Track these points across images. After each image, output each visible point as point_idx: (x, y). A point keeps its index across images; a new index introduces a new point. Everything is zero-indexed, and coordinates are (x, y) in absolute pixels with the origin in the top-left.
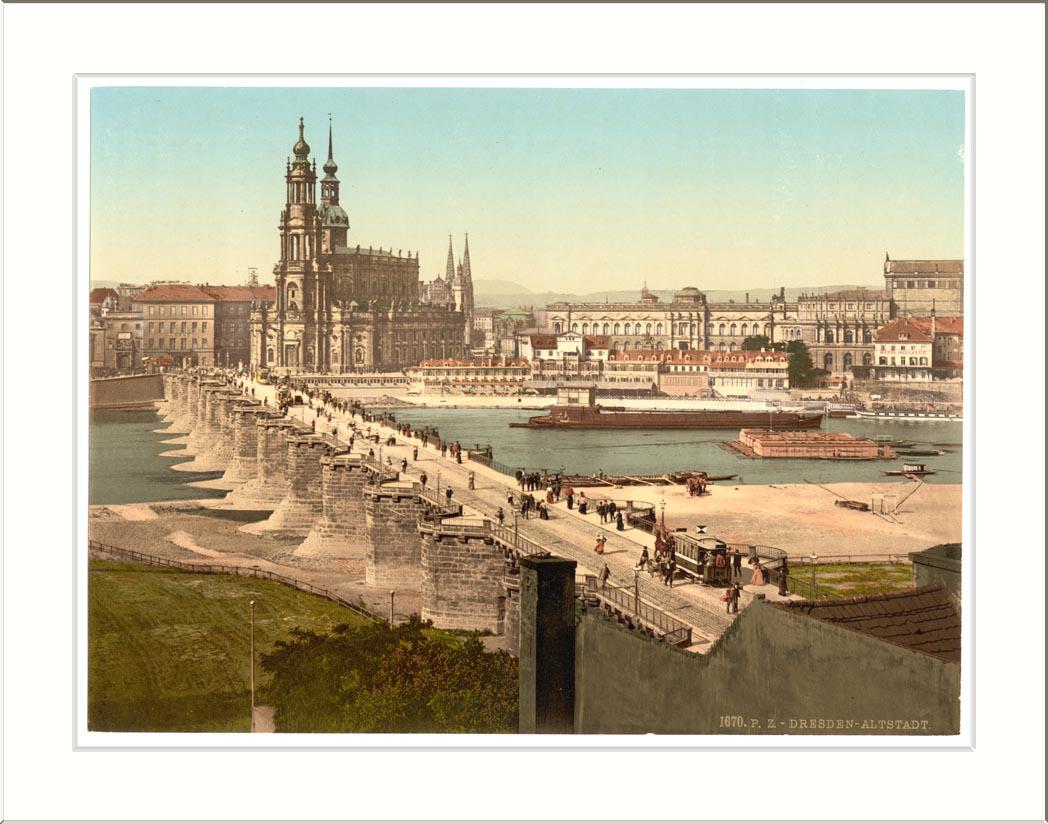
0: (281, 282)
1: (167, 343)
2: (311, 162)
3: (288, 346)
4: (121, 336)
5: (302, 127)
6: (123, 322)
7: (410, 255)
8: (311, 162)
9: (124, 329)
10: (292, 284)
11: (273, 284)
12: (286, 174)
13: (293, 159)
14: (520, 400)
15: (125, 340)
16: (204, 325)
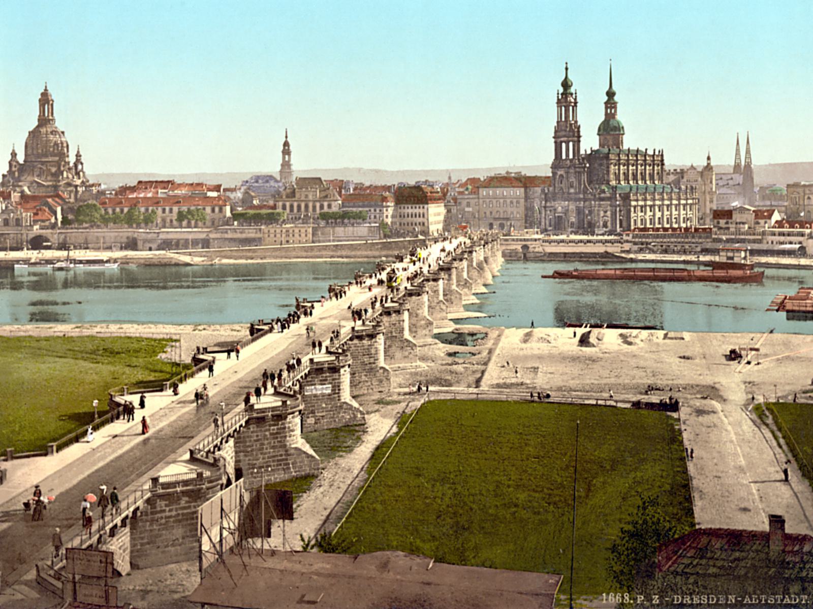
0: (554, 174)
1: (488, 213)
2: (574, 92)
3: (558, 217)
4: (467, 209)
5: (567, 69)
6: (468, 200)
7: (586, 151)
8: (574, 92)
9: (468, 205)
10: (561, 176)
11: (551, 175)
12: (556, 100)
13: (561, 90)
14: (584, 341)
15: (468, 212)
16: (518, 202)
